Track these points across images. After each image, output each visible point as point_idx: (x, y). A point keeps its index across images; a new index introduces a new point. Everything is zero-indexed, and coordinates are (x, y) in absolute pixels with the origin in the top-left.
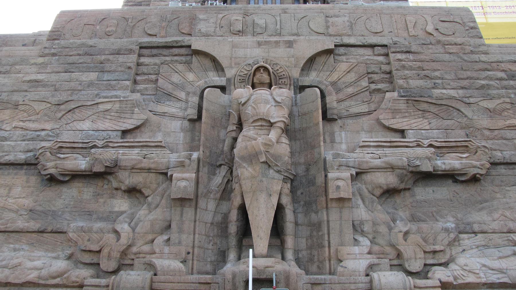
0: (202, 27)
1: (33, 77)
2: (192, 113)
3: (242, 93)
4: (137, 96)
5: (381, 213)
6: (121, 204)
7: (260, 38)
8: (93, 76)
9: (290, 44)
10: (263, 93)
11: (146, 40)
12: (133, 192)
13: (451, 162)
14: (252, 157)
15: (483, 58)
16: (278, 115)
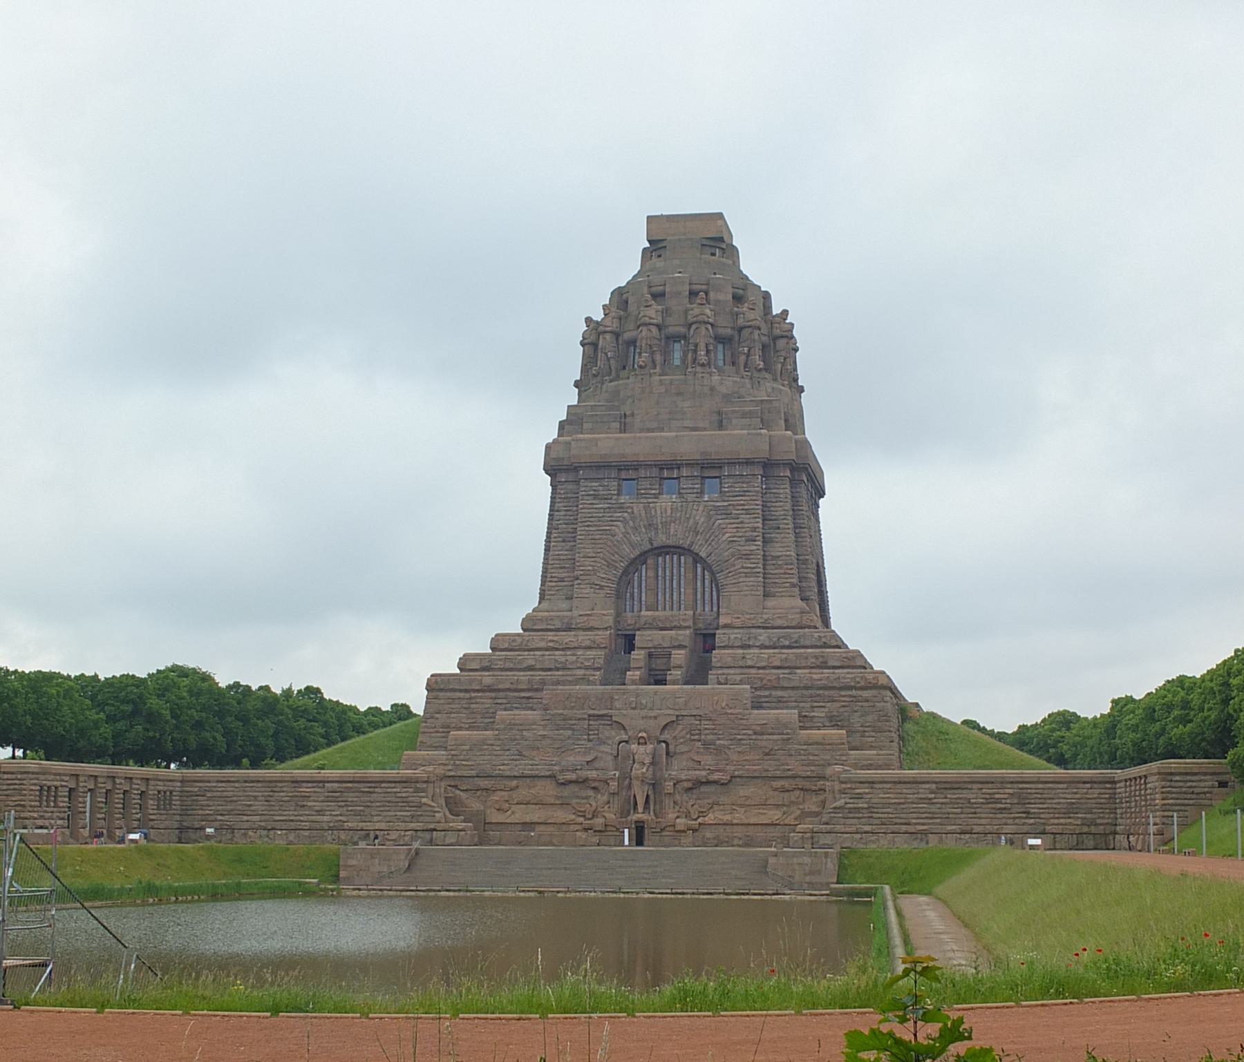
0: (617, 704)
1: (541, 733)
2: (615, 753)
3: (634, 747)
4: (590, 745)
5: (685, 797)
6: (591, 793)
7: (644, 713)
8: (570, 732)
9: (655, 718)
10: (642, 749)
11: (591, 712)
12: (594, 788)
13: (715, 777)
14: (637, 778)
15: (744, 722)
16: (647, 761)
